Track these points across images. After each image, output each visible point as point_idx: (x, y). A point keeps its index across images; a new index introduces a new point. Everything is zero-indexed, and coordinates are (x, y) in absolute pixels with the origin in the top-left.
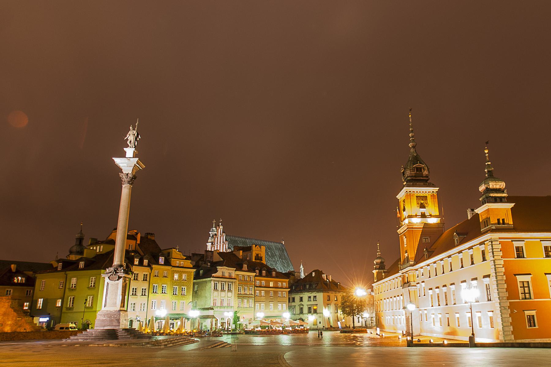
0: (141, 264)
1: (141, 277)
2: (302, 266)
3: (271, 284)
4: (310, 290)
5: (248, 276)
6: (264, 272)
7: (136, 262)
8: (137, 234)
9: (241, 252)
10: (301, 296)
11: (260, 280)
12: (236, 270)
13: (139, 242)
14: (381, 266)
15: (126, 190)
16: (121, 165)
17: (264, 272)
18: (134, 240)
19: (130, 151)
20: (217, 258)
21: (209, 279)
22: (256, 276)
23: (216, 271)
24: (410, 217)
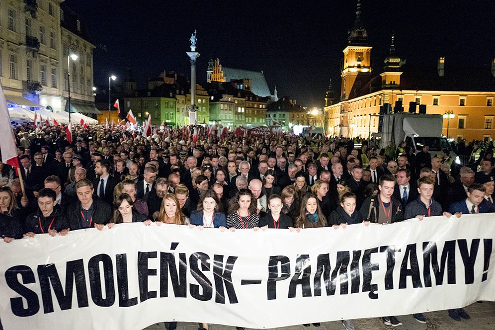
0: (180, 94)
1: (181, 102)
2: (275, 90)
3: (255, 106)
4: (282, 110)
5: (241, 101)
6: (251, 98)
7: (178, 91)
8: (175, 74)
9: (236, 84)
10: (275, 113)
11: (249, 103)
12: (234, 97)
13: (176, 79)
14: (330, 96)
15: (193, 69)
16: (190, 56)
17: (251, 98)
18: (173, 78)
19: (193, 48)
20: (221, 88)
21: (217, 102)
22: (246, 100)
23: (222, 98)
24: (349, 67)
